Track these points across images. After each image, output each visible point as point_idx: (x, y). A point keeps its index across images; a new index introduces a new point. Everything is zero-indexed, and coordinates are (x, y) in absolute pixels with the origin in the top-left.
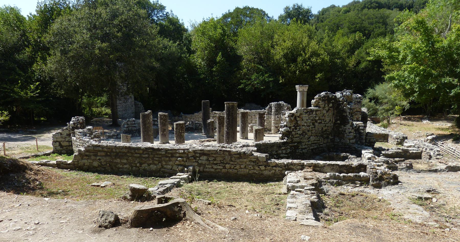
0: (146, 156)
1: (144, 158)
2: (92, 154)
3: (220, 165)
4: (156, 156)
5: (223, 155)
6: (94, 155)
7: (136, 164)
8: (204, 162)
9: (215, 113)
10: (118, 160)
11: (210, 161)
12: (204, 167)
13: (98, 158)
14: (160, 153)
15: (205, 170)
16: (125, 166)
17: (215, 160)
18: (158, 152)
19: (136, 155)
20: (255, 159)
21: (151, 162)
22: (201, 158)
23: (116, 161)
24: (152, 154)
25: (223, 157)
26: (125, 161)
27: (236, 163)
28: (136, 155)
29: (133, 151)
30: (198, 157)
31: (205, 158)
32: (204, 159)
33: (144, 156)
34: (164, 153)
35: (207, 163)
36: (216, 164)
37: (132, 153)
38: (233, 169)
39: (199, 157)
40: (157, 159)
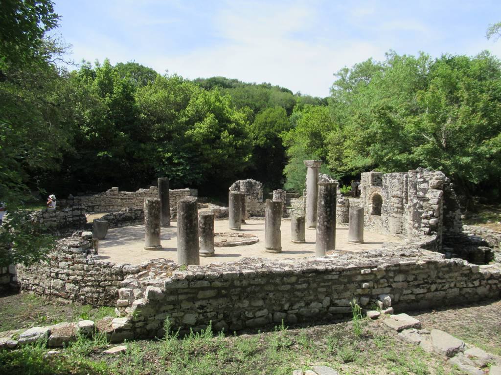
0: (304, 286)
1: (299, 290)
2: (181, 297)
3: (423, 288)
4: (322, 284)
5: (427, 270)
6: (188, 300)
7: (282, 306)
8: (399, 285)
9: (125, 194)
10: (246, 303)
11: (408, 282)
12: (401, 294)
13: (198, 304)
14: (330, 277)
15: (402, 298)
16: (259, 314)
17: (415, 279)
18: (326, 277)
19: (283, 288)
20: (468, 271)
21: (312, 297)
22: (396, 279)
23: (241, 306)
24: (314, 281)
25: (427, 273)
26: (260, 303)
27: (444, 281)
28: (283, 288)
29: (278, 280)
30: (391, 278)
31: (400, 278)
32: (401, 280)
33: (299, 287)
34: (336, 277)
35: (405, 284)
36: (418, 286)
37: (276, 285)
38: (441, 290)
39: (393, 278)
40: (323, 290)
